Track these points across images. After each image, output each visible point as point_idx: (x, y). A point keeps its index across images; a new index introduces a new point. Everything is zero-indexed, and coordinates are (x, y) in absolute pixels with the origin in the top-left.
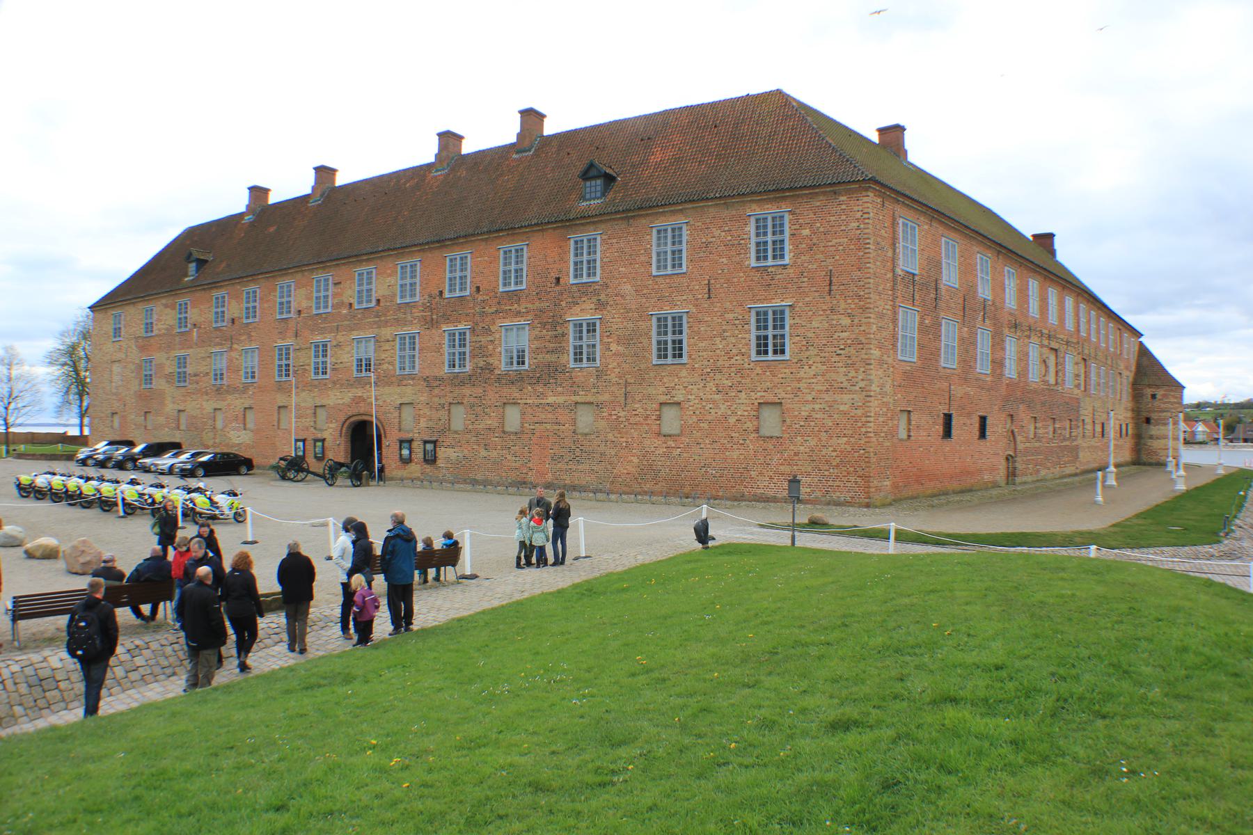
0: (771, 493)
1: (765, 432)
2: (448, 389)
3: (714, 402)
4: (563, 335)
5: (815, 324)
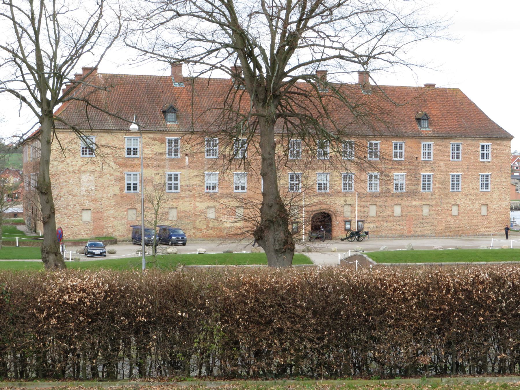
0: (484, 233)
1: (483, 214)
2: (369, 199)
3: (469, 204)
4: (419, 179)
5: (497, 180)
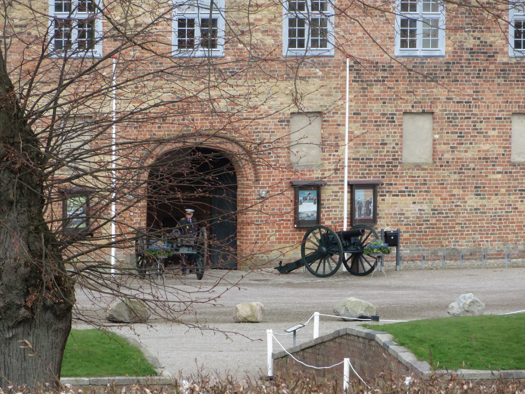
2: (402, 87)
